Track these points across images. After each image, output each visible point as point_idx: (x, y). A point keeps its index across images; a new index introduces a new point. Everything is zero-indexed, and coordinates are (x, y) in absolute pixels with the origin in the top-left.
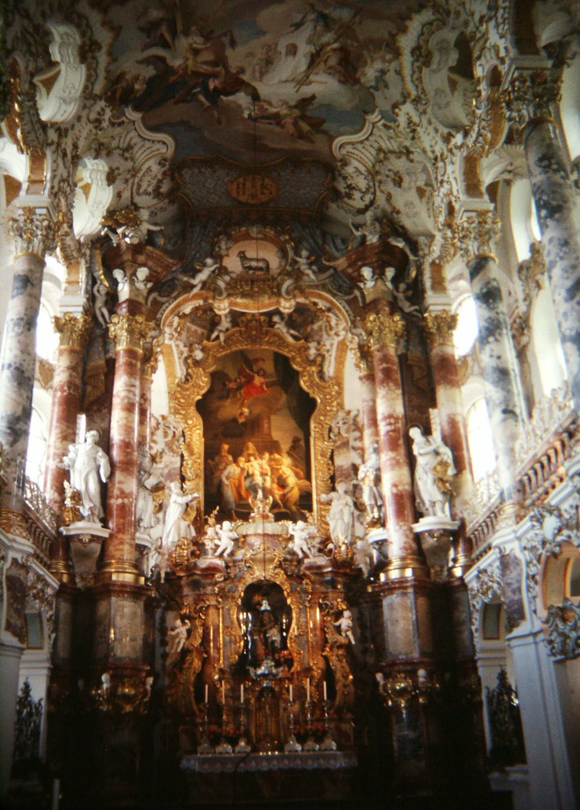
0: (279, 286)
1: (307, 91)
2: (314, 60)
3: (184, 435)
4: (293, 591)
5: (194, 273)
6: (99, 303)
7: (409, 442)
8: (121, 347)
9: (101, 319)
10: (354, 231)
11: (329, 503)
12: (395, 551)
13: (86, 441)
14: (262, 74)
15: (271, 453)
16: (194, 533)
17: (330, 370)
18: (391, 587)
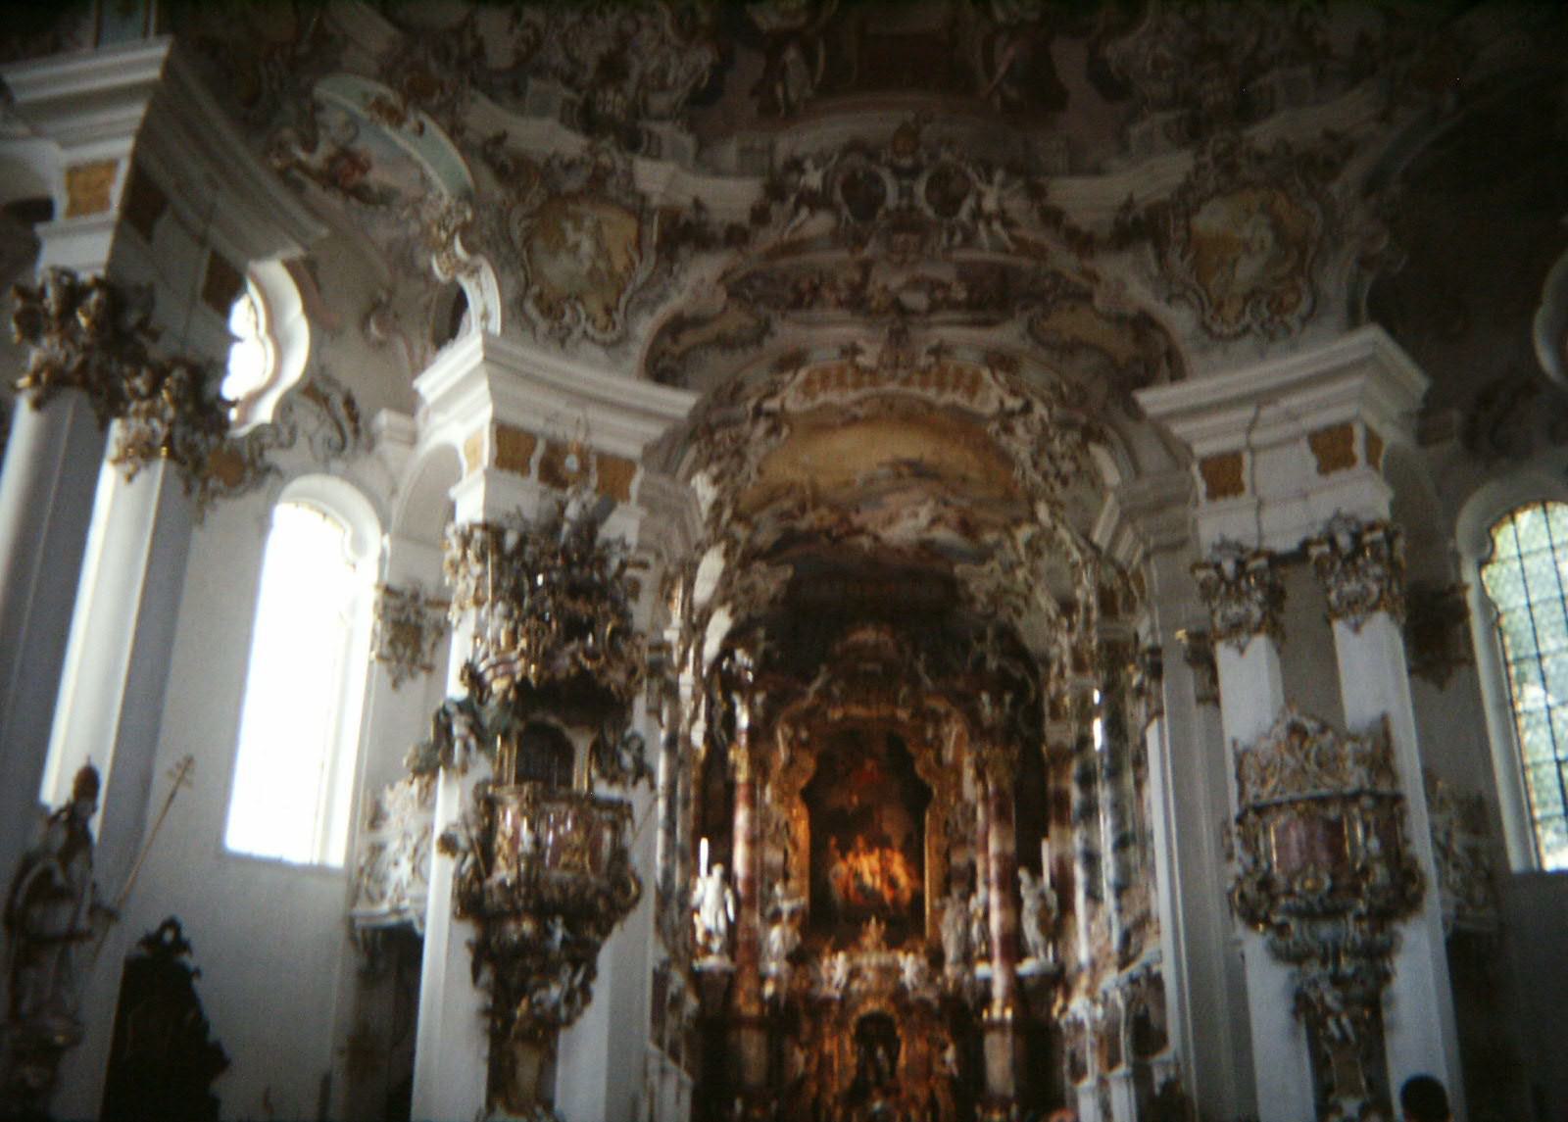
0: (896, 694)
1: (926, 536)
2: (934, 521)
3: (787, 825)
4: (903, 1022)
5: (808, 680)
6: (717, 724)
7: (1017, 883)
8: (742, 777)
9: (718, 742)
10: (975, 643)
11: (943, 908)
12: (998, 990)
13: (709, 872)
14: (883, 528)
15: (882, 849)
16: (798, 938)
17: (949, 755)
18: (993, 1026)
